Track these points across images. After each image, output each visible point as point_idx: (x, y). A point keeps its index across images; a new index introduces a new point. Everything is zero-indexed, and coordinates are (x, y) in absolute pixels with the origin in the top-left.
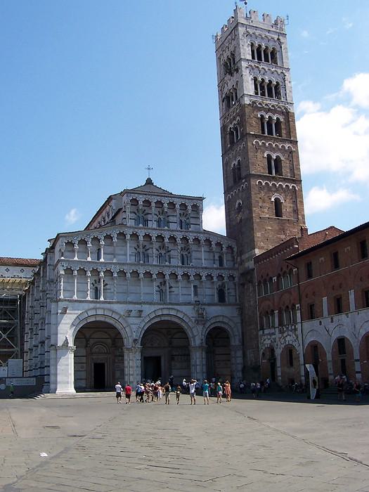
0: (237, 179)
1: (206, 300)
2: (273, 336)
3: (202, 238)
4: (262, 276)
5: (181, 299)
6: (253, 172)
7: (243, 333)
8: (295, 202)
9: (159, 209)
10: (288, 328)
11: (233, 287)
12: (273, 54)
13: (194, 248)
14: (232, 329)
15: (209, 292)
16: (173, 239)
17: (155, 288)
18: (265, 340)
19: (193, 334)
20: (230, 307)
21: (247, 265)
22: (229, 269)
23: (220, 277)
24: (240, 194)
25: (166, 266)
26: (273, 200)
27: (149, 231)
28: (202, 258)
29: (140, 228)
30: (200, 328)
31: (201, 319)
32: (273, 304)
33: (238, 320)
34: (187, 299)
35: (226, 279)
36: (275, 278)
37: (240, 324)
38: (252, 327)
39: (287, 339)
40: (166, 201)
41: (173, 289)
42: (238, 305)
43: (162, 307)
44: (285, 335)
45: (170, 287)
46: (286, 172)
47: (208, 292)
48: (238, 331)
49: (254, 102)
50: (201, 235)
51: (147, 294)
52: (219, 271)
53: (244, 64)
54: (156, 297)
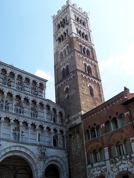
0: (65, 75)
1: (46, 144)
3: (45, 103)
4: (89, 127)
5: (30, 141)
6: (78, 69)
7: (70, 170)
8: (99, 90)
9: (19, 81)
10: (121, 158)
13: (39, 109)
14: (63, 169)
15: (47, 139)
16: (26, 100)
17: (12, 131)
18: (94, 172)
19: (36, 168)
20: (61, 151)
21: (73, 123)
22: (60, 126)
23: (55, 130)
25: (21, 116)
26: (88, 86)
27: (12, 91)
28: (44, 115)
29: (6, 87)
30: (42, 163)
31: (43, 156)
32: (103, 144)
33: (66, 160)
34: (34, 142)
35: (58, 132)
36: (104, 125)
37: (67, 163)
38: (80, 164)
39: (120, 167)
40: (24, 76)
41: (24, 134)
42: (65, 150)
43: (16, 144)
44: (117, 164)
45: (22, 132)
46: (93, 74)
47: (47, 139)
48: (66, 168)
49: (77, 38)
50: (45, 102)
51: (5, 134)
52: (54, 126)
53: (72, 21)
54: (12, 138)
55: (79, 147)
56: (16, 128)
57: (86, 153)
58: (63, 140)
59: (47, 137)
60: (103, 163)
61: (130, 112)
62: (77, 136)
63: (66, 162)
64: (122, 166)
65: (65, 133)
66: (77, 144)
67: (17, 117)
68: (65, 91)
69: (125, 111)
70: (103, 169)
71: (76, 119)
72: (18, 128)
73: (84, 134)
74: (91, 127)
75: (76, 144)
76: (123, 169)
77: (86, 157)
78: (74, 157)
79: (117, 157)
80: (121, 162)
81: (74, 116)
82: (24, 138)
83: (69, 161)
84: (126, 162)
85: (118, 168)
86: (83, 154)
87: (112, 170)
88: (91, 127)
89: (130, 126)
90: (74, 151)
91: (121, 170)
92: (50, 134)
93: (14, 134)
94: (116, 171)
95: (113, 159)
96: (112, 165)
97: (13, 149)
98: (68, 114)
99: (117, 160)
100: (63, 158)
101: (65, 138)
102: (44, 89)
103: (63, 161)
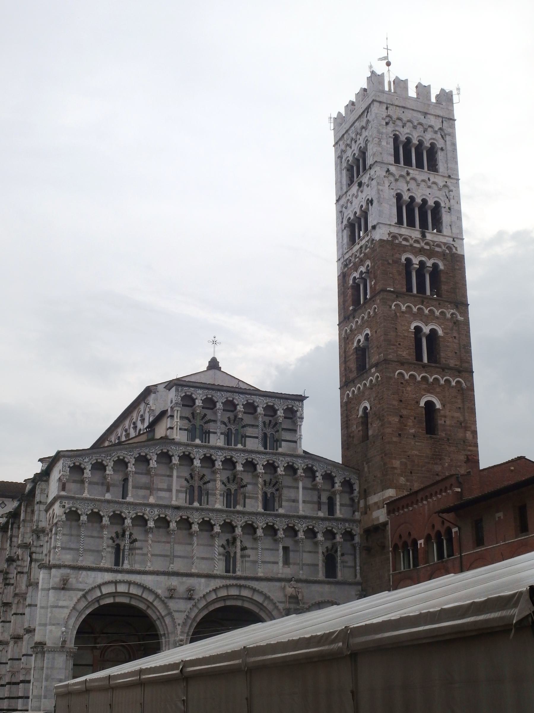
3: (300, 465)
4: (400, 537)
12: (432, 151)
16: (250, 465)
23: (330, 534)
24: (367, 393)
25: (239, 512)
27: (212, 451)
35: (339, 538)
40: (240, 401)
41: (247, 552)
45: (243, 549)
51: (203, 558)
52: (327, 524)
56: (228, 541)
61: (459, 529)
65: (357, 539)
67: (227, 516)
68: (361, 417)
71: (379, 508)
72: (235, 539)
73: (390, 553)
74: (403, 539)
82: (248, 561)
88: (403, 539)
92: (316, 544)
93: (224, 555)
97: (223, 593)
101: (358, 551)
102: (299, 423)
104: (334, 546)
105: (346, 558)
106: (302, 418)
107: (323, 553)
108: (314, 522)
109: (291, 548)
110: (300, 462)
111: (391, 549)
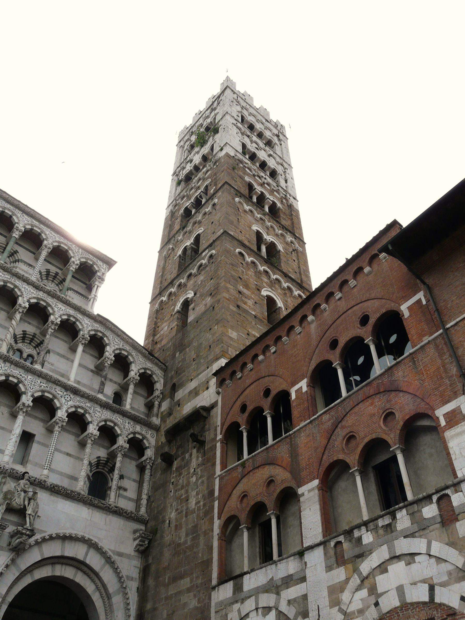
2: (293, 592)
3: (86, 327)
4: (244, 408)
10: (389, 528)
11: (135, 475)
22: (135, 419)
33: (131, 568)
37: (133, 587)
38: (185, 583)
39: (384, 582)
44: (366, 566)
52: (107, 414)
55: (192, 503)
57: (217, 523)
58: (140, 483)
59: (68, 454)
60: (289, 567)
62: (191, 460)
63: (132, 579)
64: (398, 571)
65: (149, 453)
66: (187, 492)
68: (178, 312)
69: (403, 297)
70: (289, 602)
74: (250, 408)
75: (183, 491)
76: (400, 590)
77: (216, 544)
78: (167, 554)
79: (366, 524)
80: (391, 549)
81: (193, 385)
83: (145, 572)
84: (418, 544)
85: (373, 590)
86: (205, 533)
87: (335, 602)
89: (431, 350)
90: (173, 525)
91: (390, 602)
92: (82, 445)
94: (361, 612)
95: (341, 538)
96: (340, 574)
98: (174, 381)
99: (367, 538)
100: (120, 554)
102: (97, 283)
103: (116, 570)
104: (112, 456)
105: (126, 483)
106: (103, 280)
107: (90, 464)
108: (88, 405)
109: (36, 438)
110: (87, 322)
111: (219, 437)
